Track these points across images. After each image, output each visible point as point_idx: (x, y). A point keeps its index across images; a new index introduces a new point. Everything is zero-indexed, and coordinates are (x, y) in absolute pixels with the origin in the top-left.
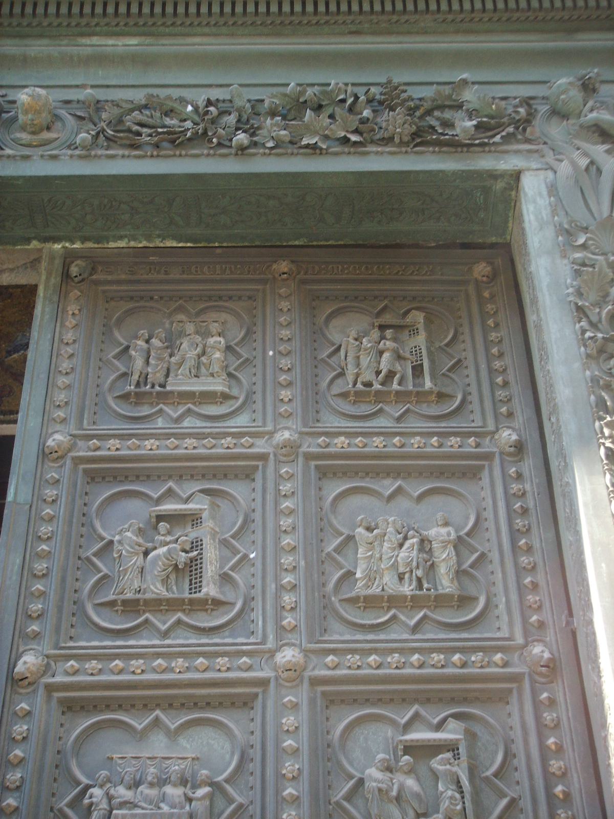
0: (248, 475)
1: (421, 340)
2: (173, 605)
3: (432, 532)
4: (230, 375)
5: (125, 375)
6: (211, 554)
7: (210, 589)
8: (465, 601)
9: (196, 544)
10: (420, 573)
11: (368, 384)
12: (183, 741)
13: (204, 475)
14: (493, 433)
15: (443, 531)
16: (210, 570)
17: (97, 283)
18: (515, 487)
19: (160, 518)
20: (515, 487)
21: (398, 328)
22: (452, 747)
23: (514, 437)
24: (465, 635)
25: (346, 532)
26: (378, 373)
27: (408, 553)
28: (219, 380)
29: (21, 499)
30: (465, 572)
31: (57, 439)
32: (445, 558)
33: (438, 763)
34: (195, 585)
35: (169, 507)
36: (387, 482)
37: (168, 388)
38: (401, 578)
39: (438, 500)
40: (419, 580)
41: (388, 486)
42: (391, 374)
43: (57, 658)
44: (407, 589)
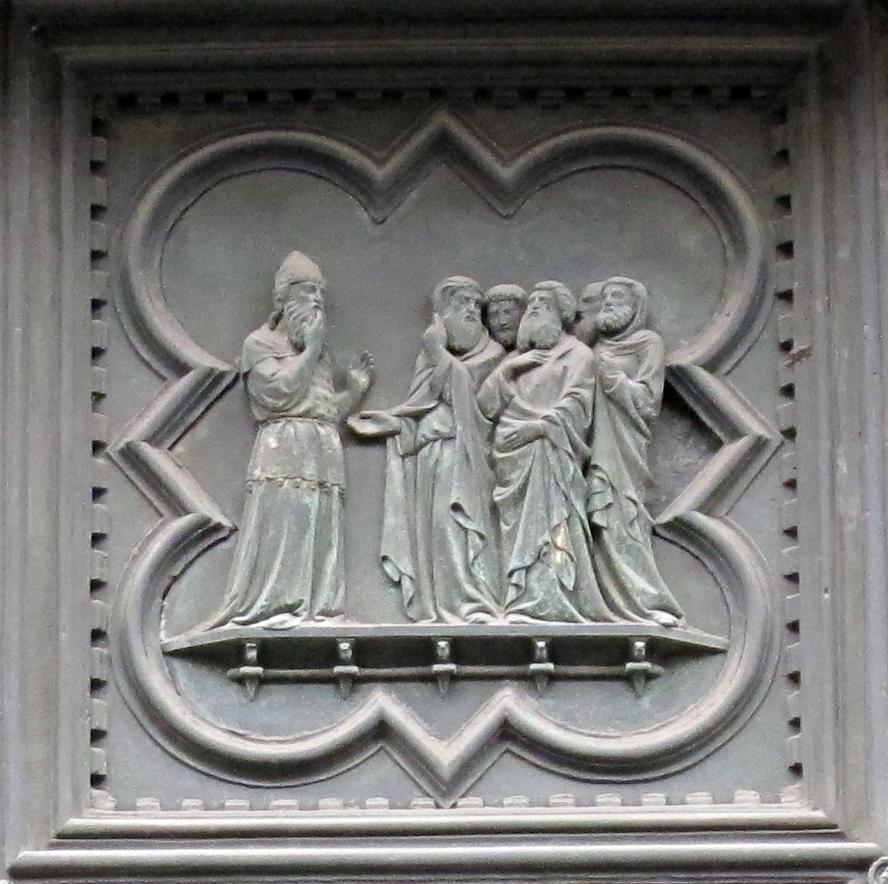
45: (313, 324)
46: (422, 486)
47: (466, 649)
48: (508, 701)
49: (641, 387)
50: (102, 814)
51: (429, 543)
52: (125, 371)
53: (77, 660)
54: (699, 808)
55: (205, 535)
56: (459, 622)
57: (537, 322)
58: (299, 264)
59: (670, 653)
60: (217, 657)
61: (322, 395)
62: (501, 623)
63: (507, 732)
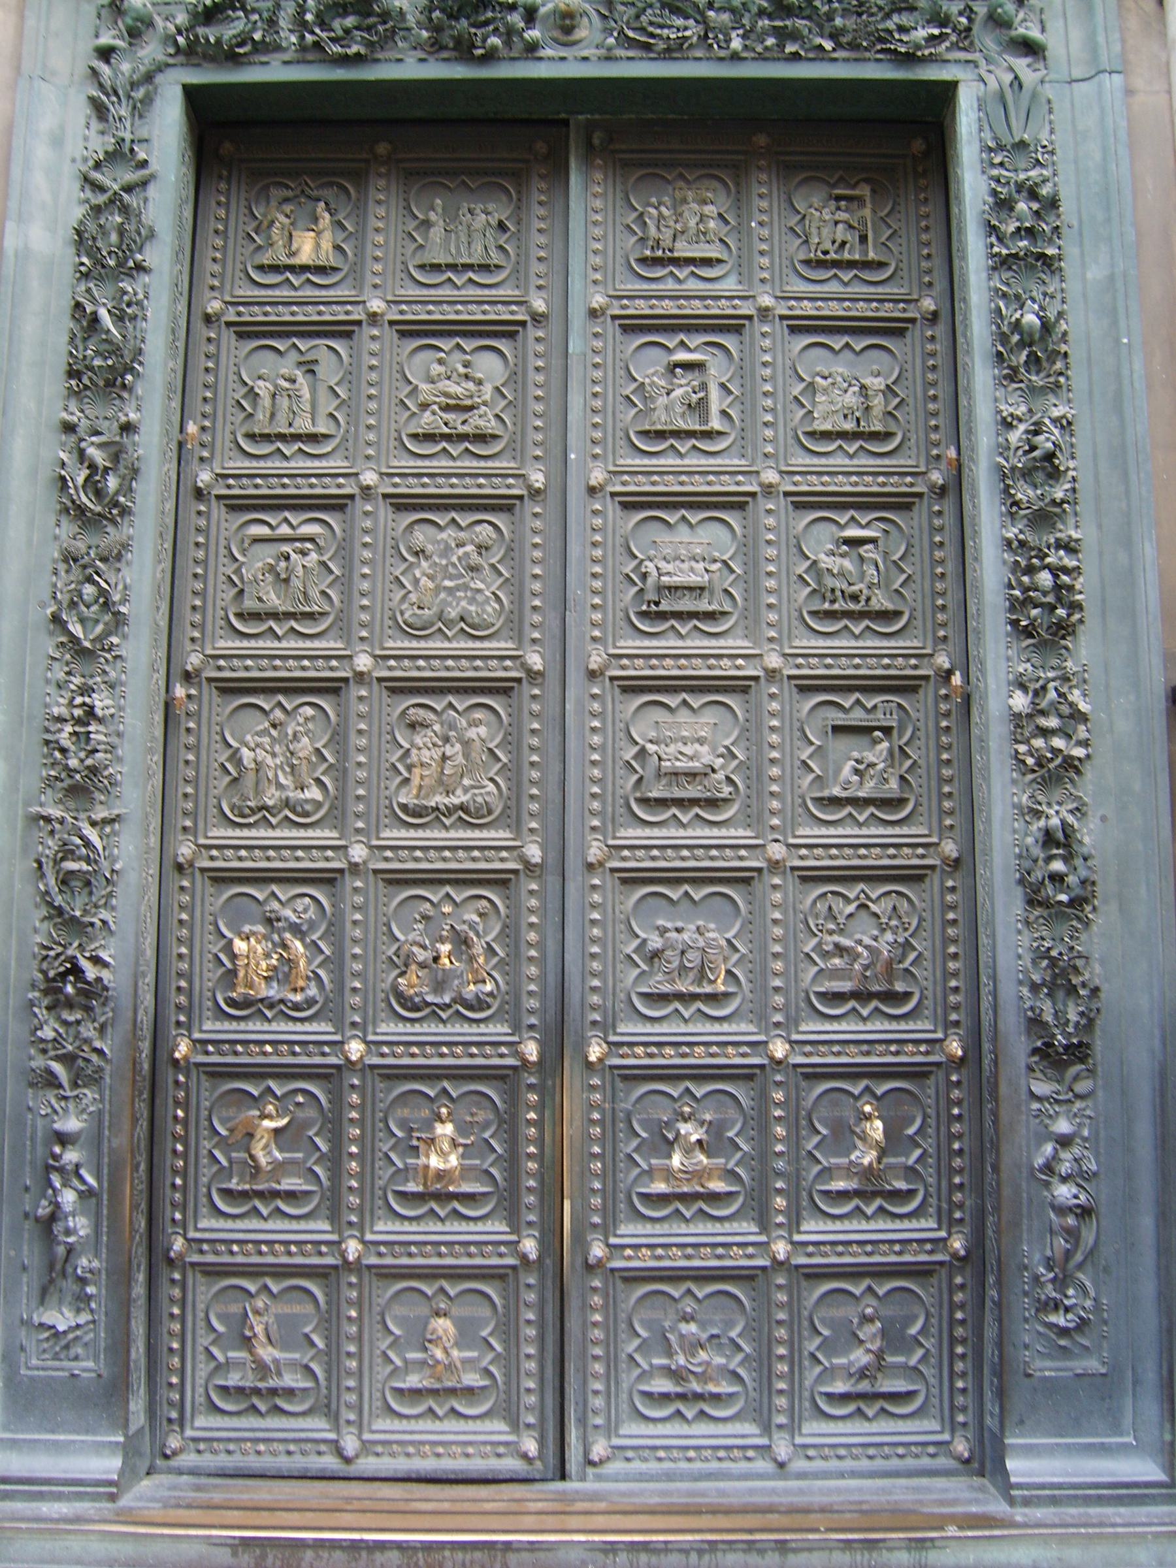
0: (737, 330)
1: (867, 212)
2: (691, 434)
3: (868, 381)
4: (721, 240)
5: (642, 239)
6: (714, 393)
7: (716, 424)
8: (887, 436)
9: (704, 386)
10: (857, 414)
11: (825, 253)
12: (700, 531)
13: (706, 329)
14: (917, 301)
15: (876, 381)
16: (714, 407)
17: (613, 152)
18: (929, 347)
19: (677, 365)
20: (929, 347)
21: (849, 199)
22: (873, 541)
23: (933, 308)
24: (893, 643)
25: (808, 379)
26: (834, 242)
27: (851, 399)
28: (712, 247)
29: (578, 350)
30: (890, 413)
31: (598, 300)
32: (878, 402)
33: (867, 551)
34: (705, 419)
35: (682, 356)
36: (837, 337)
37: (676, 254)
38: (845, 416)
39: (875, 353)
40: (858, 420)
41: (837, 342)
42: (844, 243)
43: (615, 473)
44: (849, 426)
45: (440, 210)
46: (458, 238)
47: (463, 265)
48: (471, 275)
49: (494, 222)
50: (403, 292)
51: (458, 248)
52: (408, 220)
53: (399, 266)
54: (501, 292)
55: (421, 246)
56: (462, 261)
57: (478, 211)
58: (438, 201)
59: (497, 267)
60: (422, 267)
61: (441, 223)
62: (469, 261)
63: (470, 280)
